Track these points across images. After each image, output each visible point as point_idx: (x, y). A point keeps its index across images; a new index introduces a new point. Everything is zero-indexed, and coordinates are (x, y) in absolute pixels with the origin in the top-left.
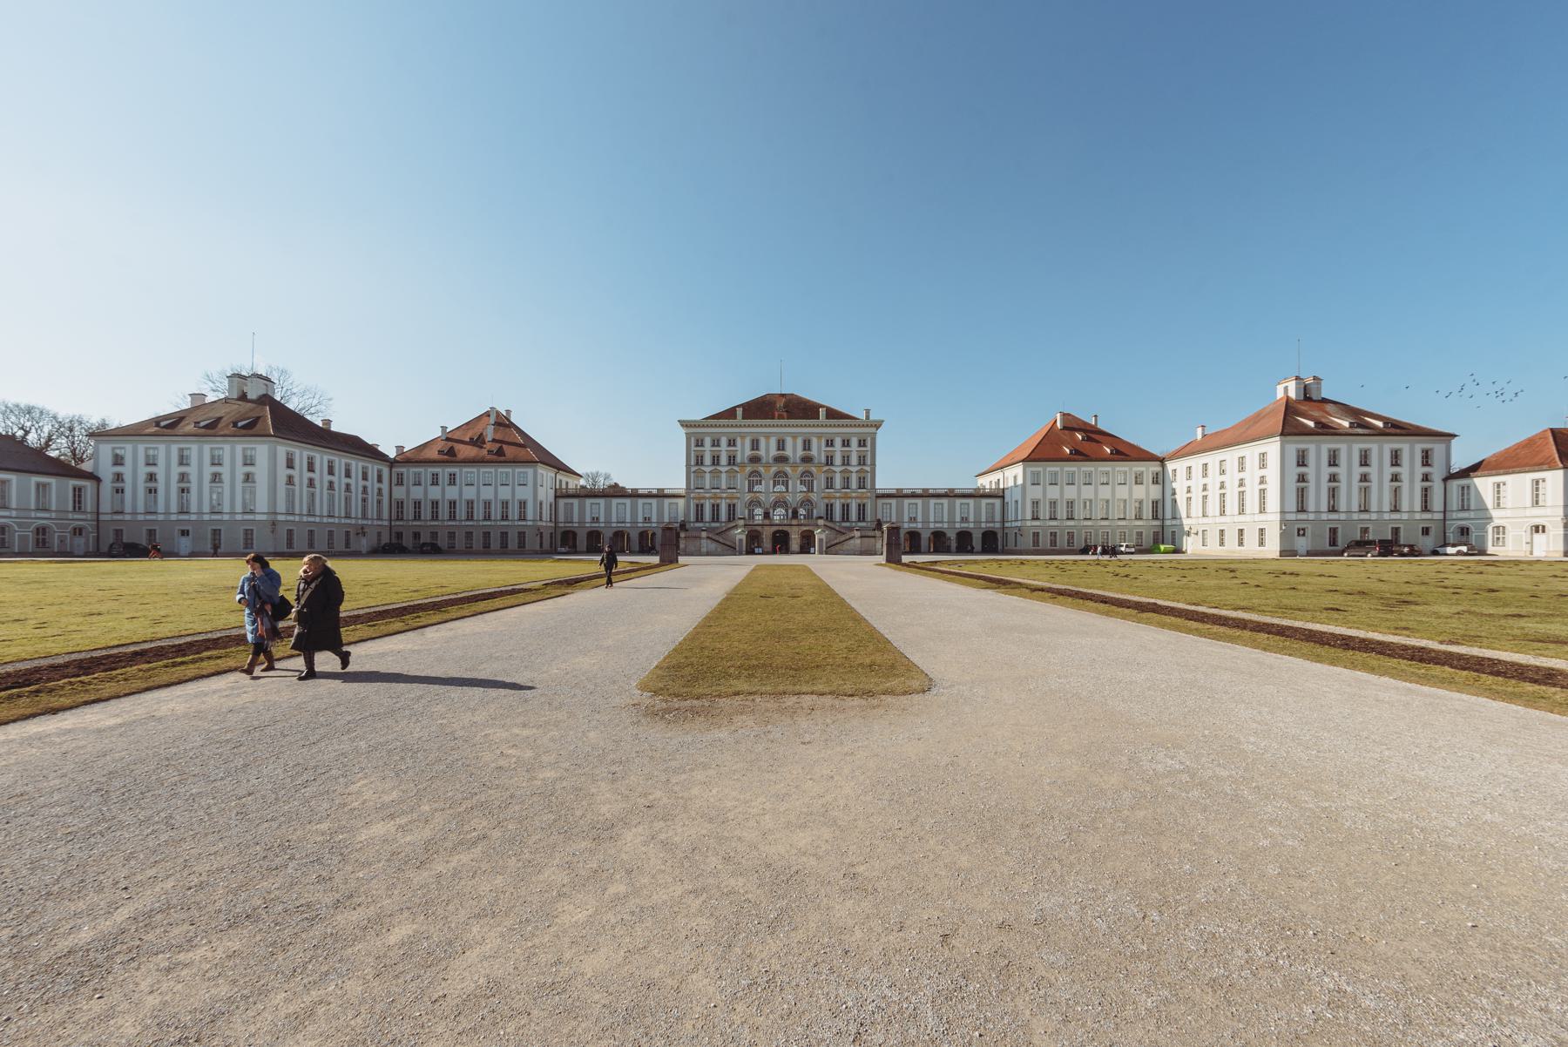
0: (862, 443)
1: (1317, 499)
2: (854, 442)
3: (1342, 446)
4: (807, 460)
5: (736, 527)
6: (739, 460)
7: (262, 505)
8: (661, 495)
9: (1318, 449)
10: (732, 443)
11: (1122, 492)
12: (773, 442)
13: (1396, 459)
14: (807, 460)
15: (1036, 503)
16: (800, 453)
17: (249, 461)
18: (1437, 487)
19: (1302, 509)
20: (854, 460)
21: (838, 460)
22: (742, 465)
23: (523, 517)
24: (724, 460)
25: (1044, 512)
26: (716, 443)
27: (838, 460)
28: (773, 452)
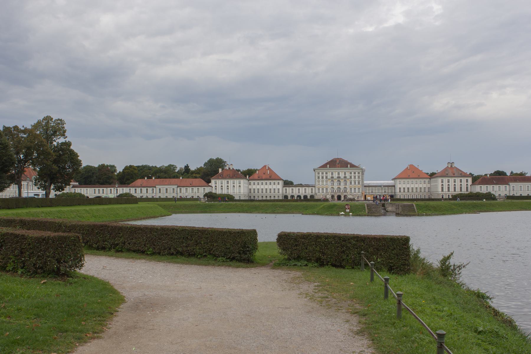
0: (359, 173)
1: (445, 189)
2: (357, 173)
3: (450, 179)
4: (345, 177)
7: (242, 192)
8: (308, 186)
9: (445, 180)
10: (326, 173)
11: (421, 186)
12: (337, 173)
13: (461, 181)
14: (345, 177)
15: (400, 188)
16: (343, 176)
17: (240, 183)
18: (469, 186)
19: (442, 191)
20: (357, 177)
21: (353, 177)
22: (329, 179)
23: (279, 192)
24: (325, 178)
25: (402, 190)
26: (323, 173)
27: (353, 177)
28: (337, 176)
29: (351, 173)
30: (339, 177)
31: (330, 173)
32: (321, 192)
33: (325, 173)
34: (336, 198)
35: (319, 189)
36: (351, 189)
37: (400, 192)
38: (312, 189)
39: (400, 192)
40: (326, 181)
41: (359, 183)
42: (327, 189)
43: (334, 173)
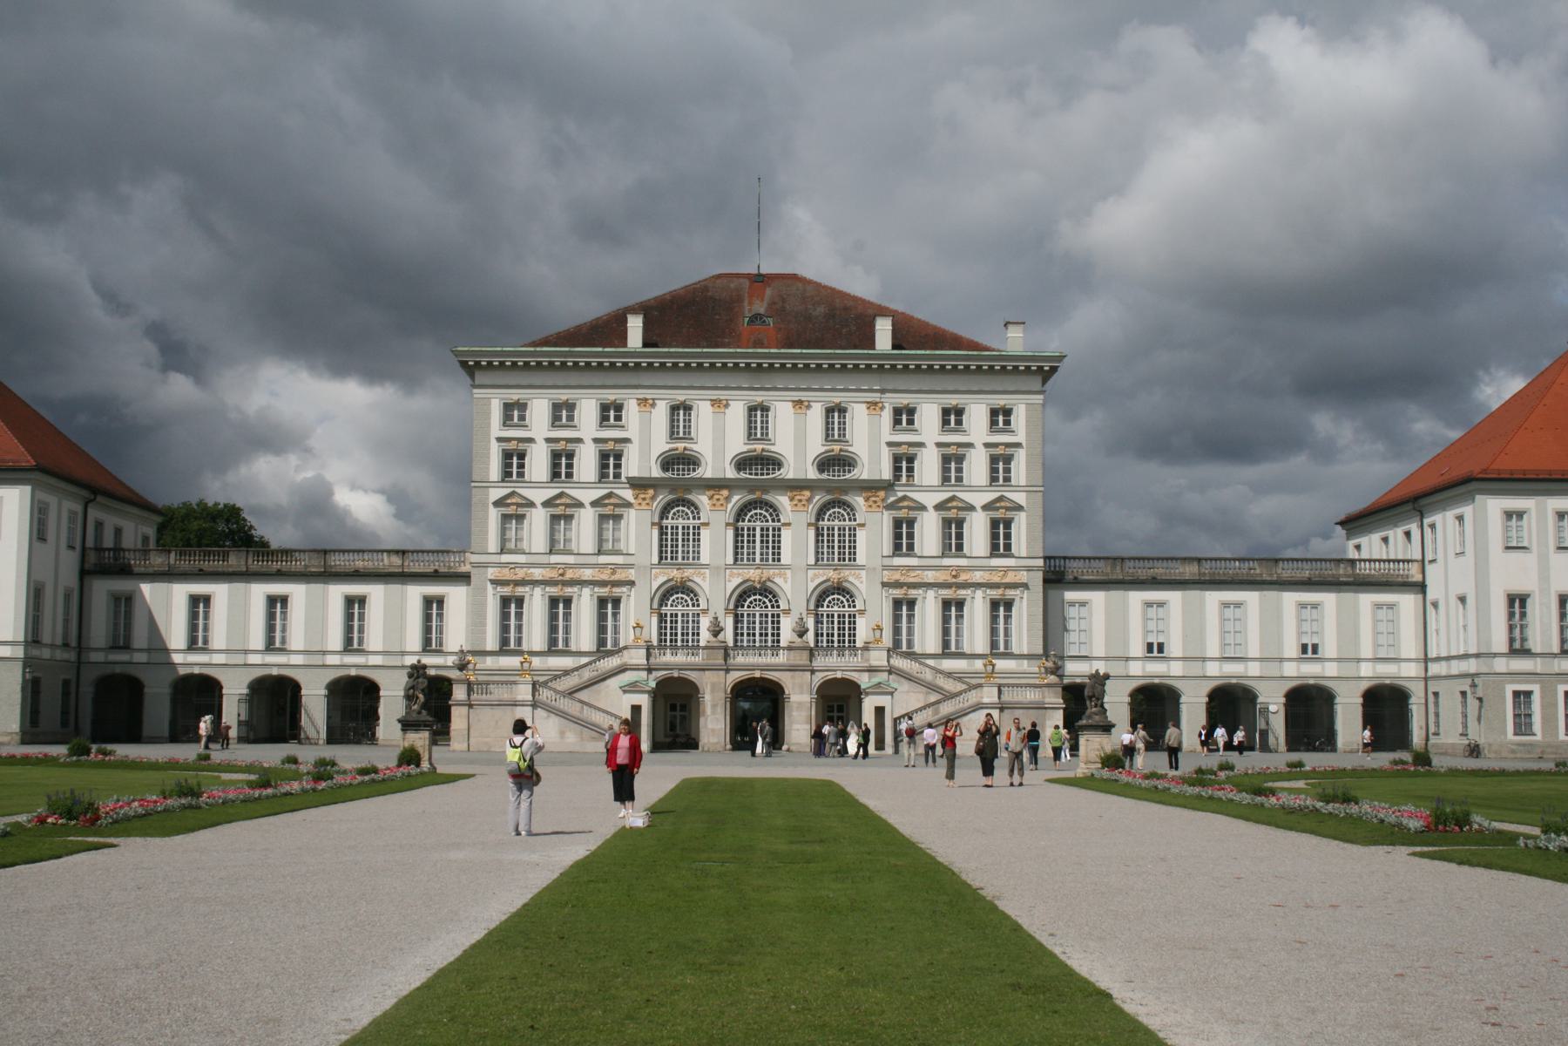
0: (999, 417)
5: (622, 670)
6: (633, 466)
10: (610, 412)
12: (737, 412)
15: (1517, 602)
16: (816, 446)
20: (977, 467)
21: (928, 467)
22: (638, 484)
24: (586, 463)
26: (562, 412)
27: (928, 467)
28: (737, 443)
29: (904, 416)
30: (758, 462)
31: (661, 412)
32: (535, 635)
33: (587, 410)
34: (714, 723)
35: (511, 605)
36: (903, 606)
37: (1518, 649)
38: (433, 605)
39: (1518, 649)
40: (609, 512)
41: (1000, 542)
42: (607, 605)
43: (703, 412)
